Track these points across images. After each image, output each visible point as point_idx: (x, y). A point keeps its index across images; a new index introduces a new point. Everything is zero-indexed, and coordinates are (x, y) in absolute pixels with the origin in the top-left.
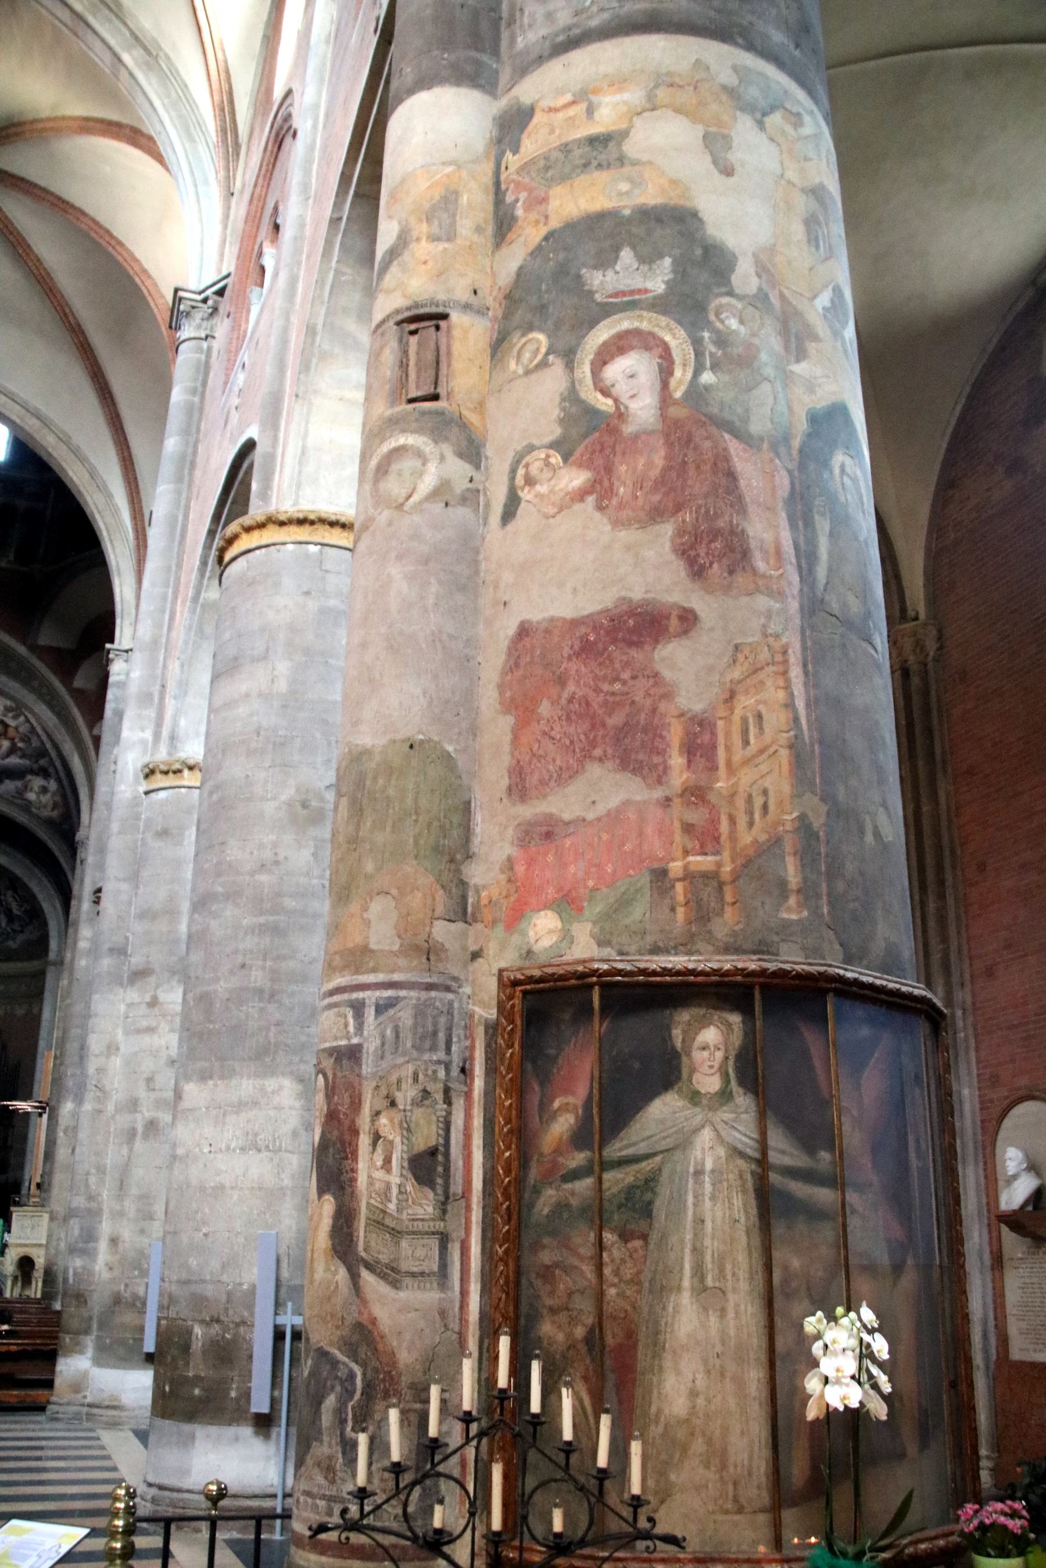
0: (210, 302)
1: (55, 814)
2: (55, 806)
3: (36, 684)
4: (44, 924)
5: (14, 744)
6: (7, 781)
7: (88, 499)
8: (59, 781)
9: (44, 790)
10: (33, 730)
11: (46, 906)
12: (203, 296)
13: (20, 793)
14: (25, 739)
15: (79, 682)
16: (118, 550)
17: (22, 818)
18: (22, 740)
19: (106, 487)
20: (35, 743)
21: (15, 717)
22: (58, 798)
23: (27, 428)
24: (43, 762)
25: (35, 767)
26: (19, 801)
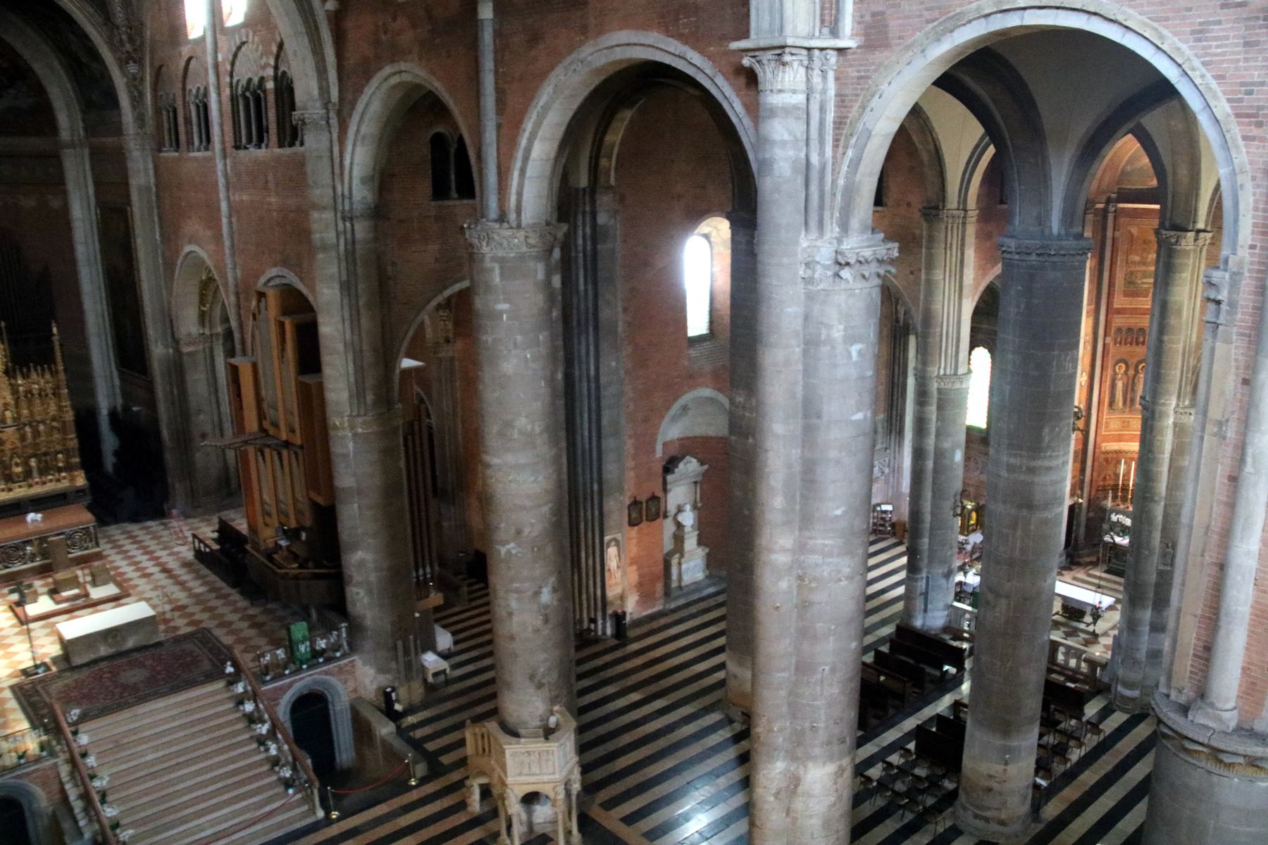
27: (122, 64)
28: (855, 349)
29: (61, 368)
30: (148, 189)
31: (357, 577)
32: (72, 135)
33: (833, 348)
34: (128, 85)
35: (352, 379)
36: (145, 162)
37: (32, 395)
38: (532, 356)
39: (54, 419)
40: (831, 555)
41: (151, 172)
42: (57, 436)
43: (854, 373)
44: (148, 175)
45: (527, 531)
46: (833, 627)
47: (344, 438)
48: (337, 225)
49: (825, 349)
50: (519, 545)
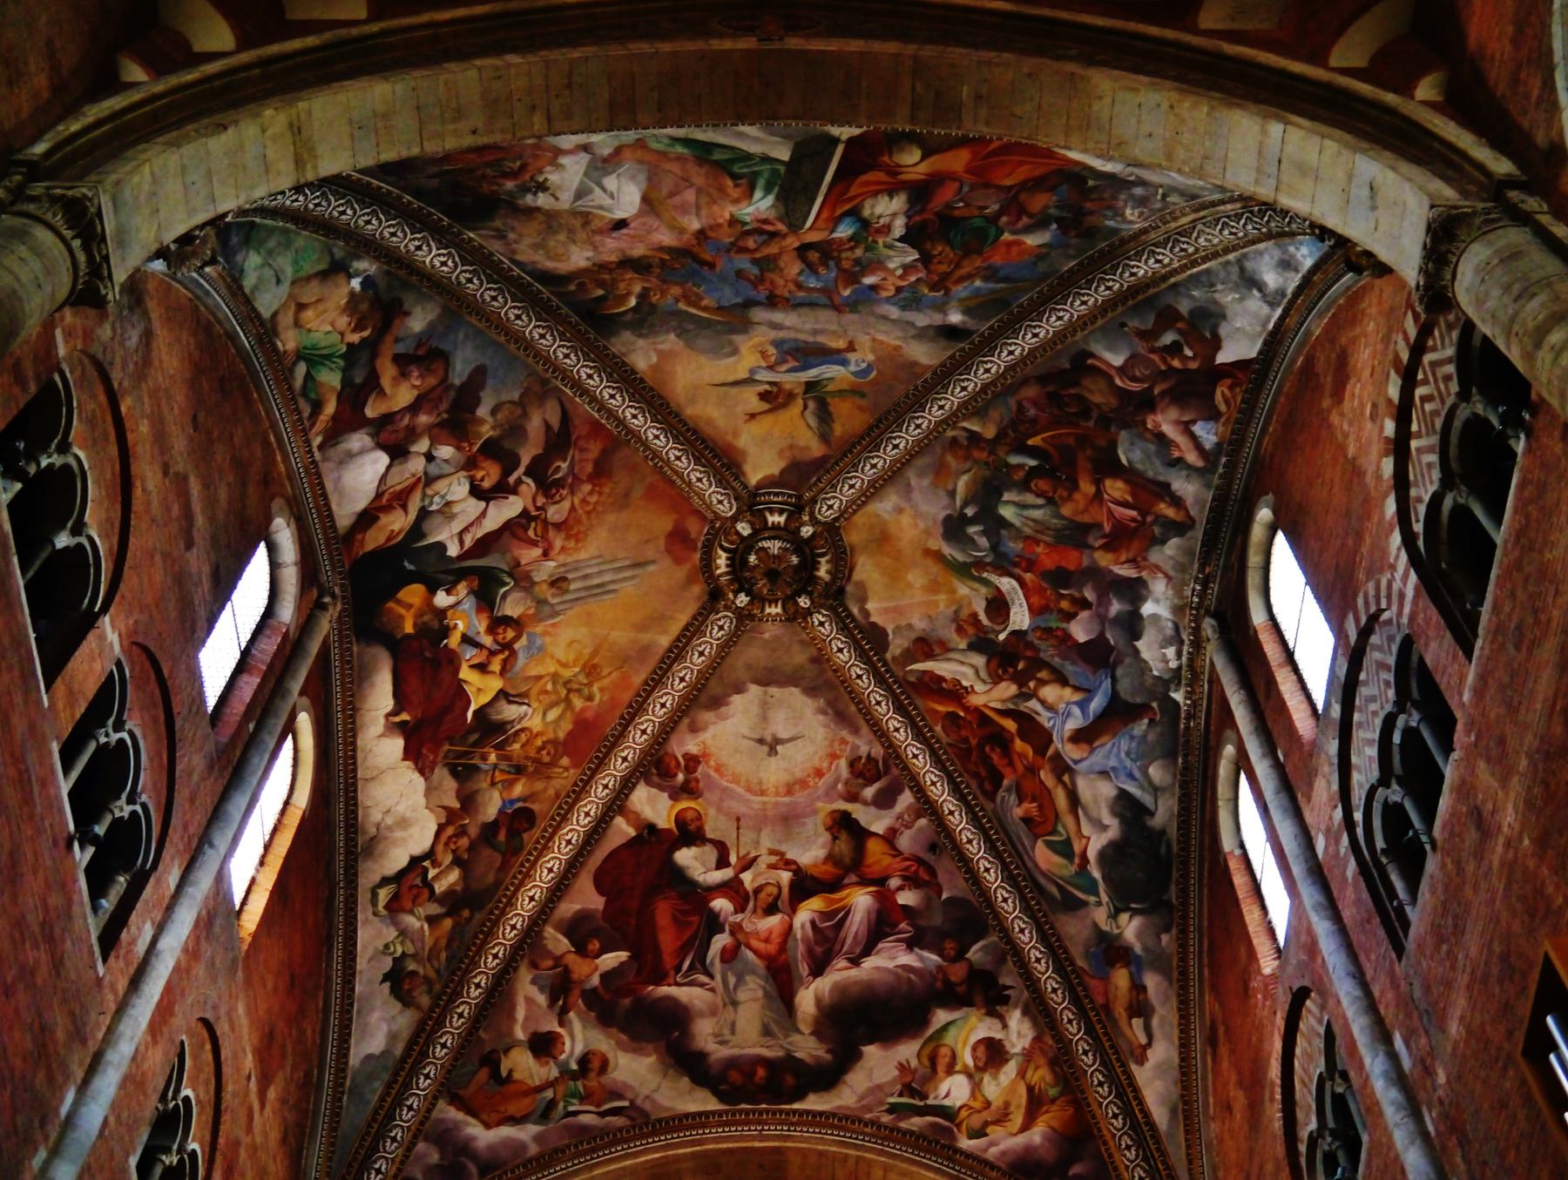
2: (1036, 1103)
5: (884, 899)
6: (871, 1051)
8: (1039, 1011)
9: (993, 1053)
10: (942, 840)
18: (911, 881)
20: (952, 887)
21: (885, 800)
22: (1040, 1075)
24: (975, 953)
25: (957, 972)
26: (915, 1123)
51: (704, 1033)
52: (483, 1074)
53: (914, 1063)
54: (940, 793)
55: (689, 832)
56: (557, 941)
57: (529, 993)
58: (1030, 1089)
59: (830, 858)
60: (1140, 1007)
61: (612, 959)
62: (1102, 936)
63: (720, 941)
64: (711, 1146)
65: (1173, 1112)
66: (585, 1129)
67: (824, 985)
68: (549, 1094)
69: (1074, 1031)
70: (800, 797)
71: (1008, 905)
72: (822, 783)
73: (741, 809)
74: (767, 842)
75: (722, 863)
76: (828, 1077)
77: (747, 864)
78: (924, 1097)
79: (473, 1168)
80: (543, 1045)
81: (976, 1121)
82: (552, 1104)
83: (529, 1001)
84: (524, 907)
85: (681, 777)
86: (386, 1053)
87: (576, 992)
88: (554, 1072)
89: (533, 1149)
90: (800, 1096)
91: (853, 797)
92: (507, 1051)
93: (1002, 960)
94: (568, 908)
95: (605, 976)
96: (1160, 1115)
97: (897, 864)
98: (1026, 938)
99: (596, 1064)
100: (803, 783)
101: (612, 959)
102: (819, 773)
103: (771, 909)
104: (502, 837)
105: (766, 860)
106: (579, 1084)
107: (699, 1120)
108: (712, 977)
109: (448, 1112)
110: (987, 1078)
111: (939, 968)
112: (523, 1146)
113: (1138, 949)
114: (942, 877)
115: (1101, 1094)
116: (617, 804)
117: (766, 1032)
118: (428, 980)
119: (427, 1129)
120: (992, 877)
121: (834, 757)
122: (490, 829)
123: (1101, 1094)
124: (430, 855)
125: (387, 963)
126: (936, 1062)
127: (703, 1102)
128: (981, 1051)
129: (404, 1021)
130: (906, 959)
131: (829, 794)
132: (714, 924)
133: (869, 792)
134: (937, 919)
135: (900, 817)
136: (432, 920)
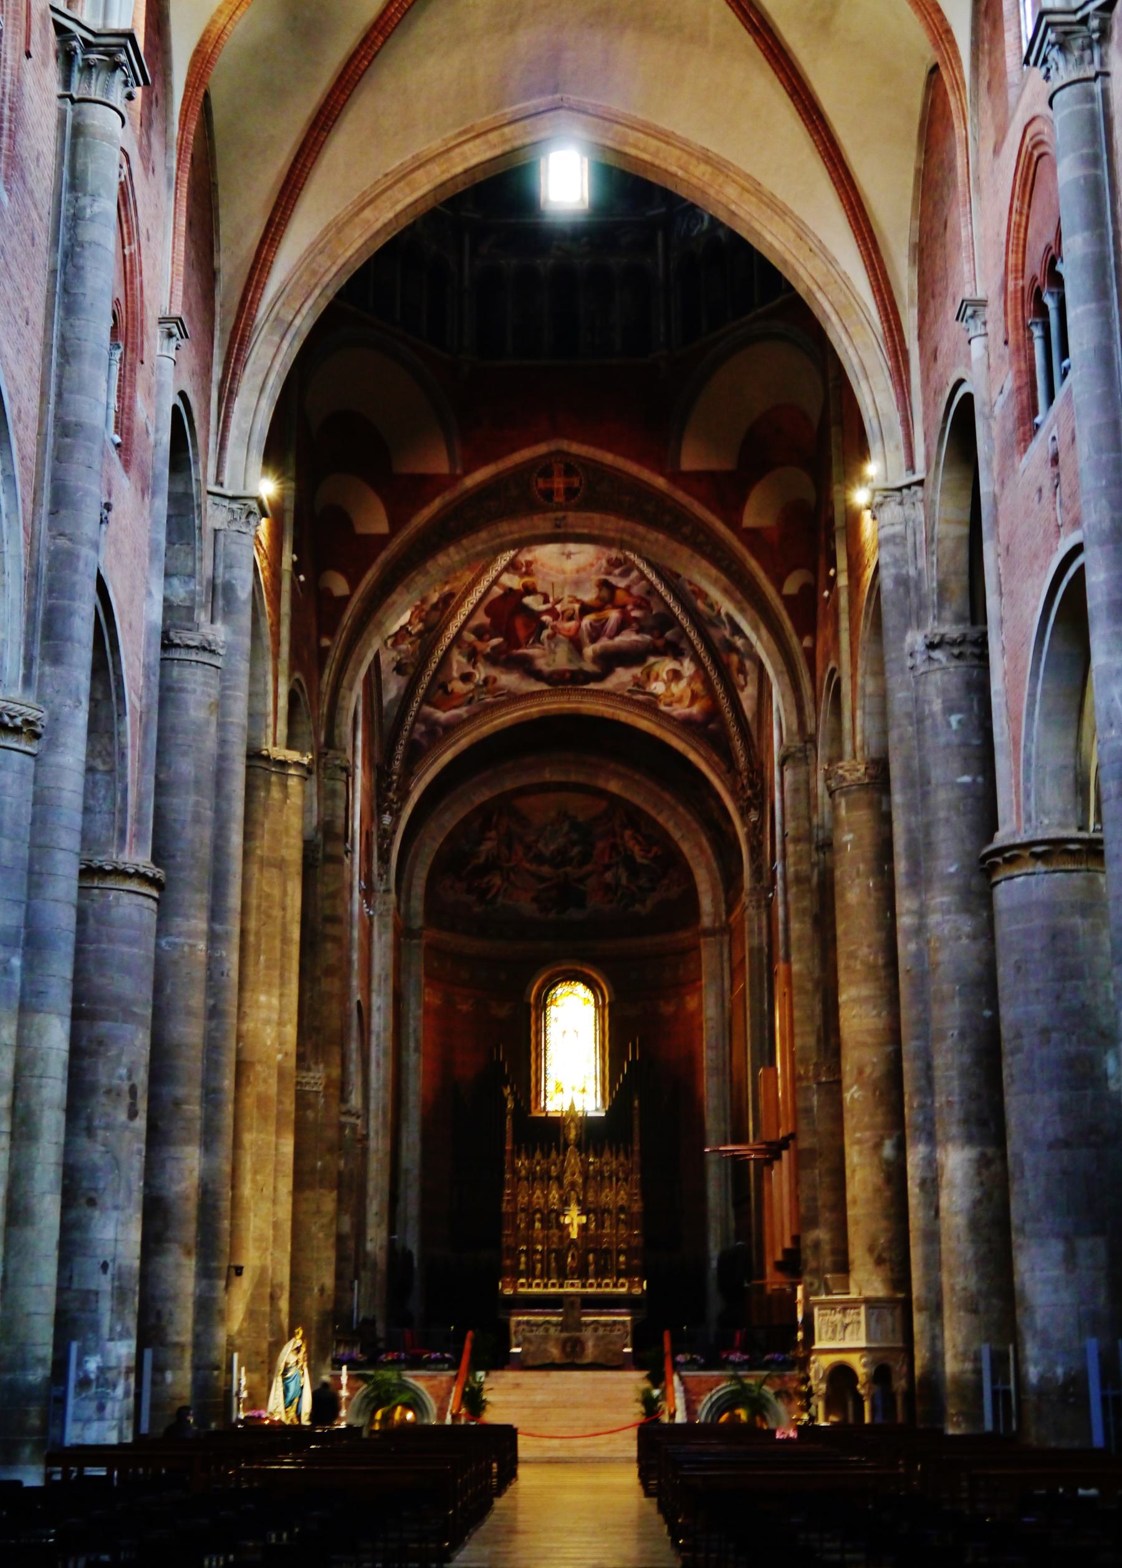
0: (1094, 23)
1: (695, 710)
2: (694, 698)
3: (687, 530)
4: (688, 875)
5: (625, 614)
6: (620, 671)
7: (801, 271)
8: (696, 659)
9: (676, 675)
10: (652, 590)
11: (685, 847)
12: (1080, 15)
13: (640, 685)
14: (642, 603)
15: (750, 519)
16: (857, 341)
17: (645, 724)
18: (637, 606)
19: (824, 250)
20: (656, 609)
21: (625, 574)
22: (698, 687)
23: (694, 181)
24: (669, 634)
25: (660, 643)
26: (640, 697)
27: (744, 813)
28: (954, 719)
29: (636, 1148)
30: (760, 949)
31: (812, 1264)
32: (714, 921)
33: (934, 720)
34: (748, 836)
35: (818, 1021)
36: (760, 920)
37: (603, 1177)
38: (874, 884)
39: (622, 1209)
40: (949, 912)
41: (765, 931)
42: (623, 1231)
43: (956, 740)
44: (760, 933)
45: (868, 1070)
46: (957, 988)
47: (809, 1088)
48: (810, 856)
49: (928, 723)
50: (861, 1087)
51: (541, 664)
52: (440, 692)
53: (639, 675)
54: (652, 577)
55: (529, 590)
56: (469, 637)
57: (458, 661)
58: (693, 692)
59: (598, 598)
60: (742, 670)
61: (495, 641)
62: (726, 641)
63: (546, 633)
64: (545, 707)
65: (754, 716)
66: (488, 703)
67: (597, 646)
68: (471, 695)
69: (714, 675)
70: (583, 575)
71: (686, 623)
72: (594, 569)
73: (554, 580)
74: (567, 593)
75: (546, 601)
76: (600, 677)
77: (558, 601)
78: (644, 688)
79: (440, 730)
80: (466, 678)
81: (668, 700)
82: (472, 698)
83: (458, 662)
84: (453, 630)
85: (524, 569)
86: (396, 697)
87: (480, 658)
88: (471, 686)
89: (465, 716)
90: (587, 683)
91: (609, 573)
92: (450, 682)
93: (681, 637)
94: (474, 623)
95: (494, 648)
96: (749, 714)
97: (631, 600)
98: (693, 635)
99: (491, 680)
100: (584, 569)
101: (495, 641)
102: (592, 565)
103: (570, 619)
104: (440, 605)
105: (566, 599)
106: (484, 689)
107: (540, 693)
108: (543, 644)
109: (427, 709)
110: (673, 685)
111: (652, 642)
112: (459, 716)
113: (742, 649)
114: (653, 604)
115: (724, 703)
116: (495, 582)
117: (570, 661)
118: (412, 664)
119: (416, 719)
120: (677, 610)
121: (598, 559)
122: (435, 607)
123: (724, 703)
124: (410, 623)
125: (394, 664)
126: (648, 676)
127: (541, 686)
128: (671, 675)
129: (403, 681)
130: (635, 637)
131: (598, 572)
132: (544, 626)
133: (617, 571)
134: (650, 622)
135: (632, 581)
136: (411, 643)
